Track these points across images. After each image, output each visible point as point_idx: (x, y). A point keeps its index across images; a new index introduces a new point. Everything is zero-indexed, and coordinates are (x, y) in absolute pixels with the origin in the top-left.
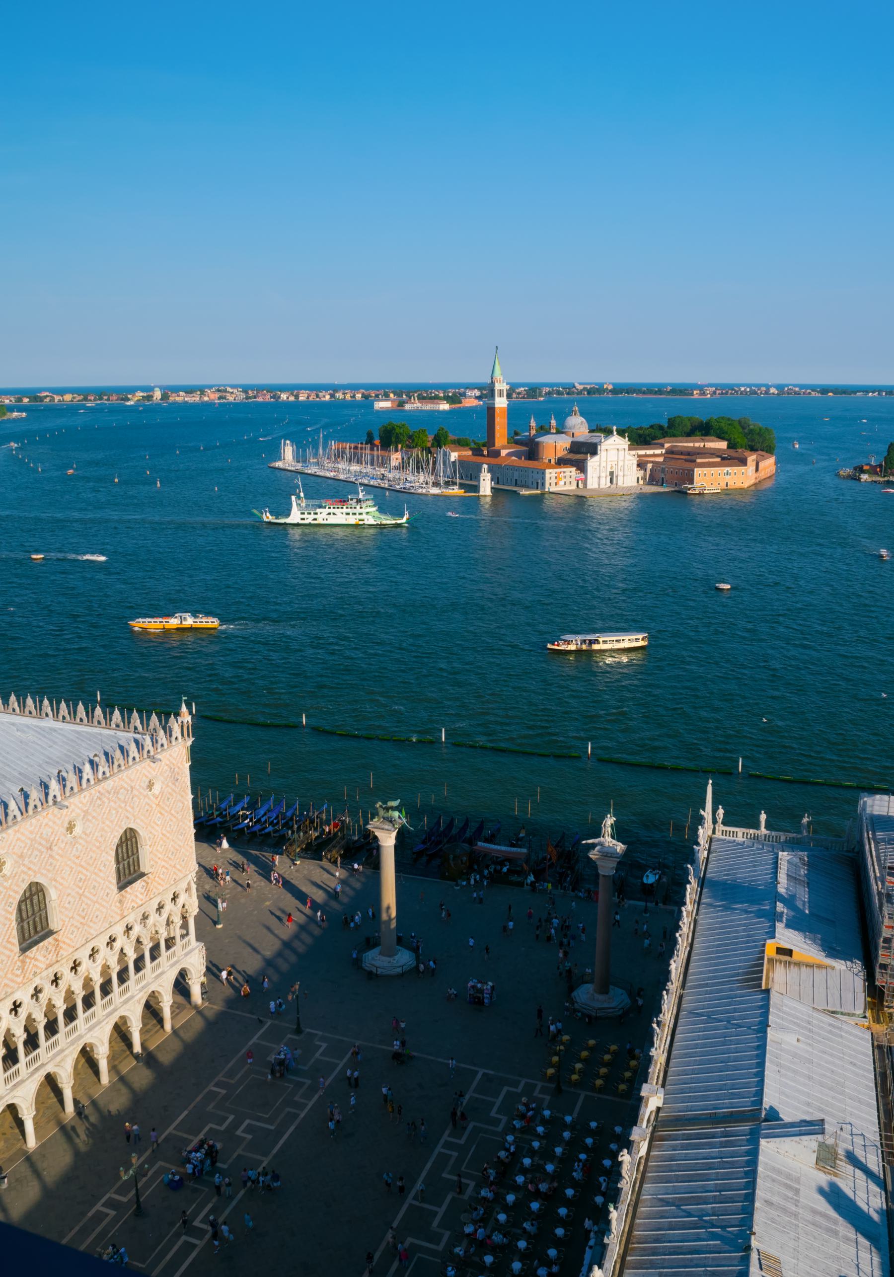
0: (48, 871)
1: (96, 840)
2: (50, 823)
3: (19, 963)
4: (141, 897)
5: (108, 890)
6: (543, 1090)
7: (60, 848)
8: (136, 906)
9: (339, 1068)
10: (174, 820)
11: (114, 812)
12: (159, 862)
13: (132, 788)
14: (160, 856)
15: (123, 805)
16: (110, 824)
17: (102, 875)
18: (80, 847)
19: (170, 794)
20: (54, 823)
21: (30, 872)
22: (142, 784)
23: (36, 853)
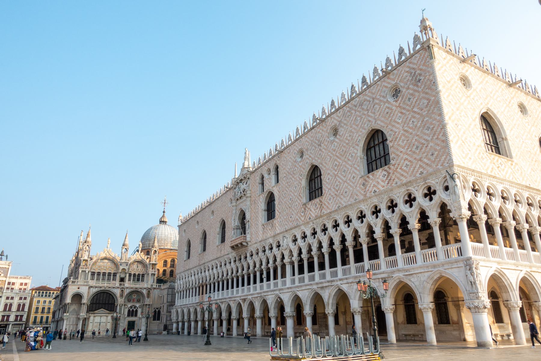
0: (318, 158)
1: (346, 139)
2: (321, 131)
3: (303, 209)
4: (383, 184)
5: (354, 175)
7: (325, 145)
11: (359, 118)
13: (373, 99)
14: (402, 150)
15: (366, 113)
16: (356, 127)
17: (350, 163)
18: (336, 144)
19: (412, 95)
20: (323, 130)
21: (310, 159)
22: (382, 94)
23: (313, 148)
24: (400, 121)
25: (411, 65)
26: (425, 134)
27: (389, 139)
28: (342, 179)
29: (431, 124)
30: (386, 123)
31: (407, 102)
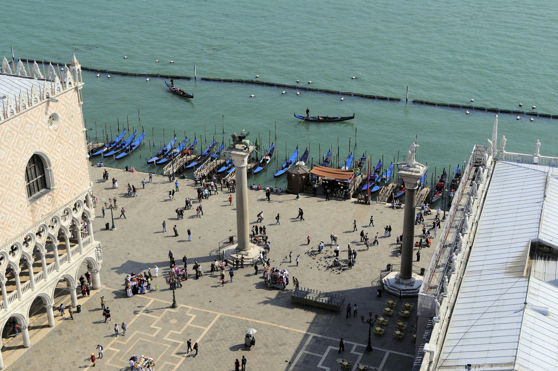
1: (10, 165)
4: (49, 207)
5: (21, 203)
6: (358, 349)
8: (44, 214)
9: (205, 333)
10: (72, 148)
11: (22, 142)
12: (61, 180)
13: (36, 123)
14: (62, 176)
15: (29, 136)
16: (19, 151)
17: (15, 191)
24: (59, 150)
25: (66, 99)
26: (76, 163)
27: (53, 166)
28: (7, 210)
29: (80, 155)
30: (48, 151)
31: (64, 133)
